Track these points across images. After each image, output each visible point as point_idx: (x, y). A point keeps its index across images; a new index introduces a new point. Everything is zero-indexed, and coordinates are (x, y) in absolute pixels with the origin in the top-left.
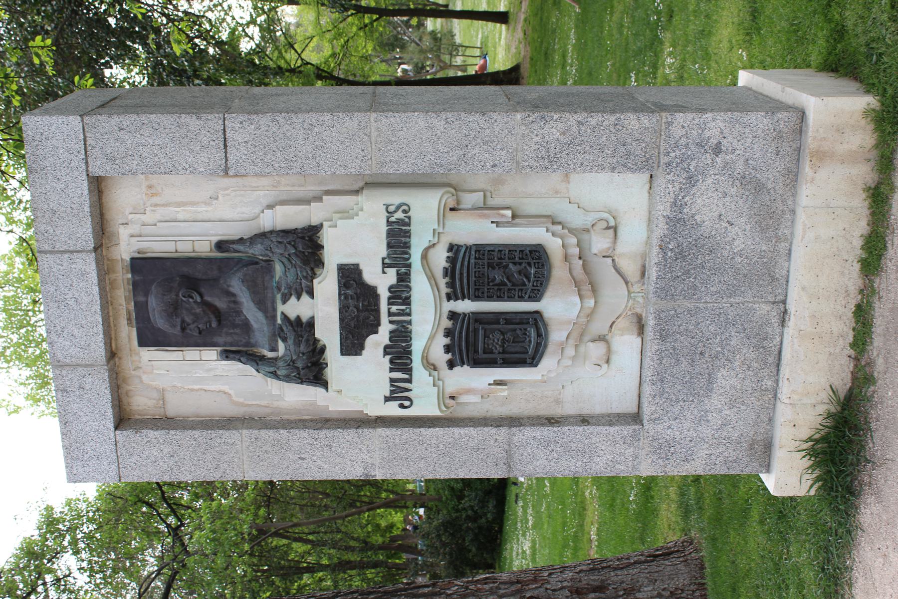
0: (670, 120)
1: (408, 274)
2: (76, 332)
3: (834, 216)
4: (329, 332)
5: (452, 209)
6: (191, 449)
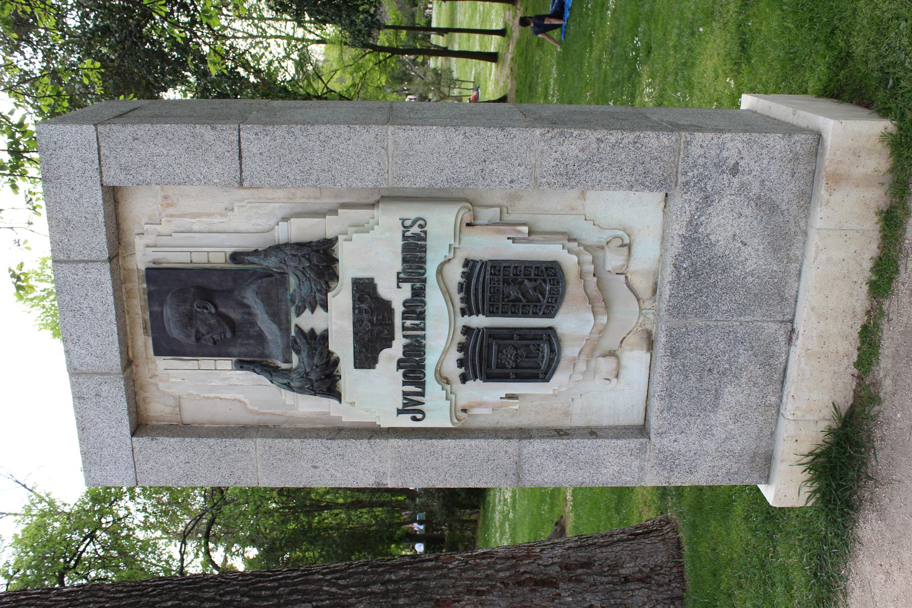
0: (689, 139)
1: (423, 289)
2: (92, 341)
3: (846, 238)
4: (342, 345)
5: (468, 225)
6: (206, 456)
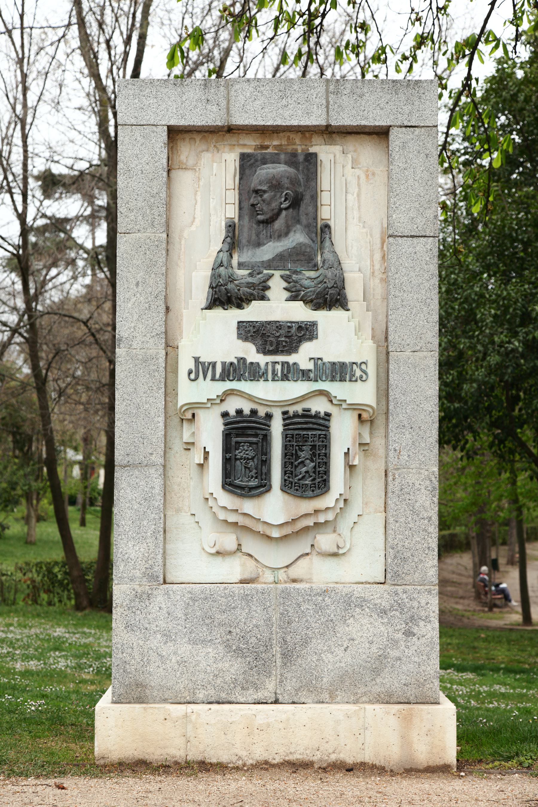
0: (433, 592)
1: (309, 379)
2: (257, 102)
3: (357, 734)
4: (255, 312)
5: (360, 416)
6: (148, 189)
